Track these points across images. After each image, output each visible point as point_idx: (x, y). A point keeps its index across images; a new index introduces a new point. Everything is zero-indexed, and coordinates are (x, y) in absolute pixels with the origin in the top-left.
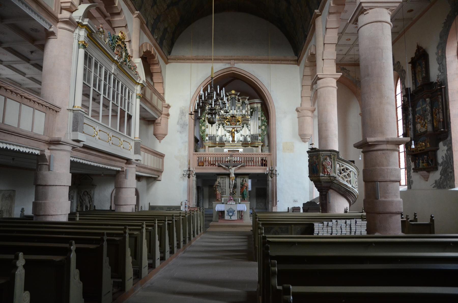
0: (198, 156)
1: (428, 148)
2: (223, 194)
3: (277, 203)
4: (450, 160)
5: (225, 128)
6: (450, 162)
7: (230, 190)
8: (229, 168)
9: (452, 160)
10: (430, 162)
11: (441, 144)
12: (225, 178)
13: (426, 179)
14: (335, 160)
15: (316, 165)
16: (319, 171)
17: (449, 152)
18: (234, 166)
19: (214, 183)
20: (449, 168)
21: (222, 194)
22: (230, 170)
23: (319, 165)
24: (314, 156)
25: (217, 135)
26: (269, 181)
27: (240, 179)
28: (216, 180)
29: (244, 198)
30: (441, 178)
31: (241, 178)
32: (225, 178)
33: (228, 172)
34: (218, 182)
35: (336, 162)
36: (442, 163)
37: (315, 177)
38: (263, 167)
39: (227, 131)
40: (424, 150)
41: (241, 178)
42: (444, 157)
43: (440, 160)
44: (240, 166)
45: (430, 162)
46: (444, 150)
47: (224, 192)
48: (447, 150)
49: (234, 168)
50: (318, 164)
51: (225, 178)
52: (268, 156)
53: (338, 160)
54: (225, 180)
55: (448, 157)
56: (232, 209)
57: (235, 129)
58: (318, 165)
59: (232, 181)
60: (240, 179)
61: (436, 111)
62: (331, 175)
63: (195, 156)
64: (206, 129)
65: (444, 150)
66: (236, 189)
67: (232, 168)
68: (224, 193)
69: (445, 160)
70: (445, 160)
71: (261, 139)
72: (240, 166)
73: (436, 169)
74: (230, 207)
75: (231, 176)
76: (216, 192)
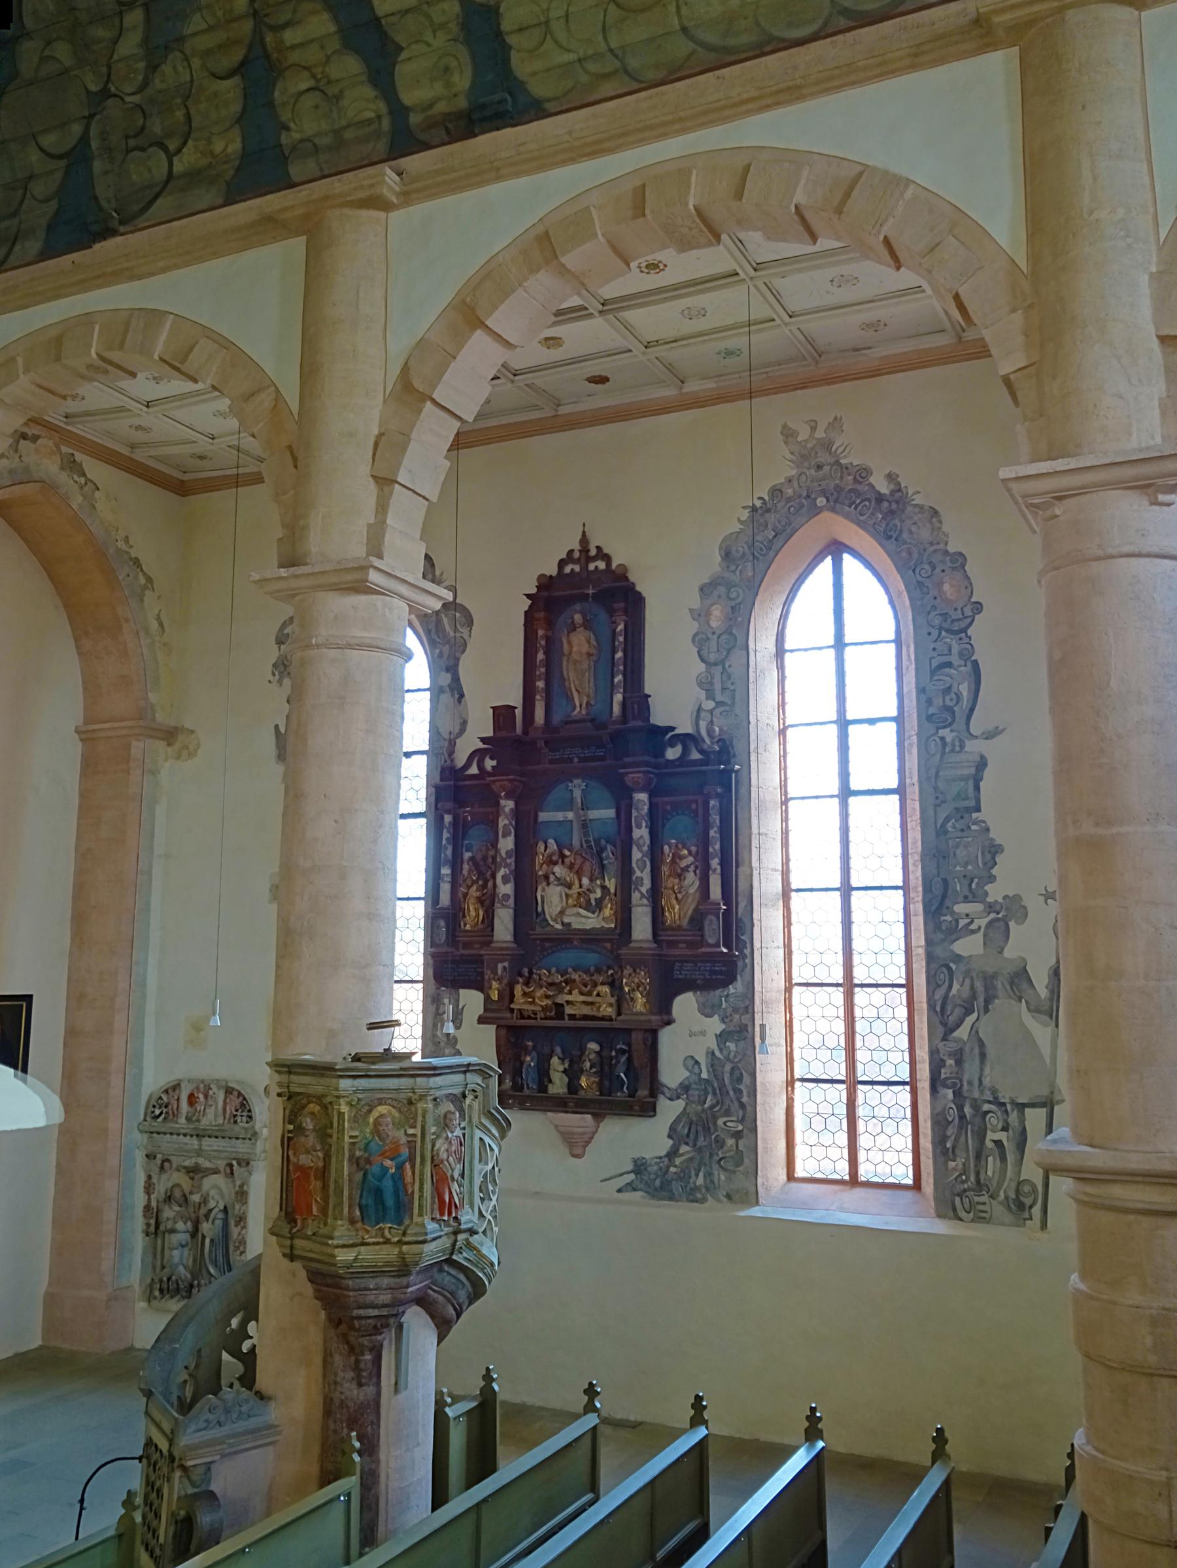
1: (637, 1014)
4: (740, 1080)
6: (739, 1092)
9: (747, 1079)
10: (622, 1075)
11: (685, 1004)
13: (576, 1145)
14: (475, 1120)
15: (400, 1167)
16: (416, 1211)
17: (731, 1046)
20: (727, 1113)
23: (418, 1160)
24: (381, 1102)
30: (672, 1154)
35: (478, 1134)
36: (685, 1088)
37: (387, 1242)
40: (610, 1019)
42: (697, 1062)
43: (671, 1073)
45: (622, 1075)
46: (703, 1033)
48: (722, 1037)
50: (412, 1159)
53: (485, 1121)
55: (728, 1067)
58: (408, 1165)
61: (677, 857)
62: (463, 1220)
65: (703, 1033)
69: (704, 1075)
70: (704, 1075)
73: (648, 1110)
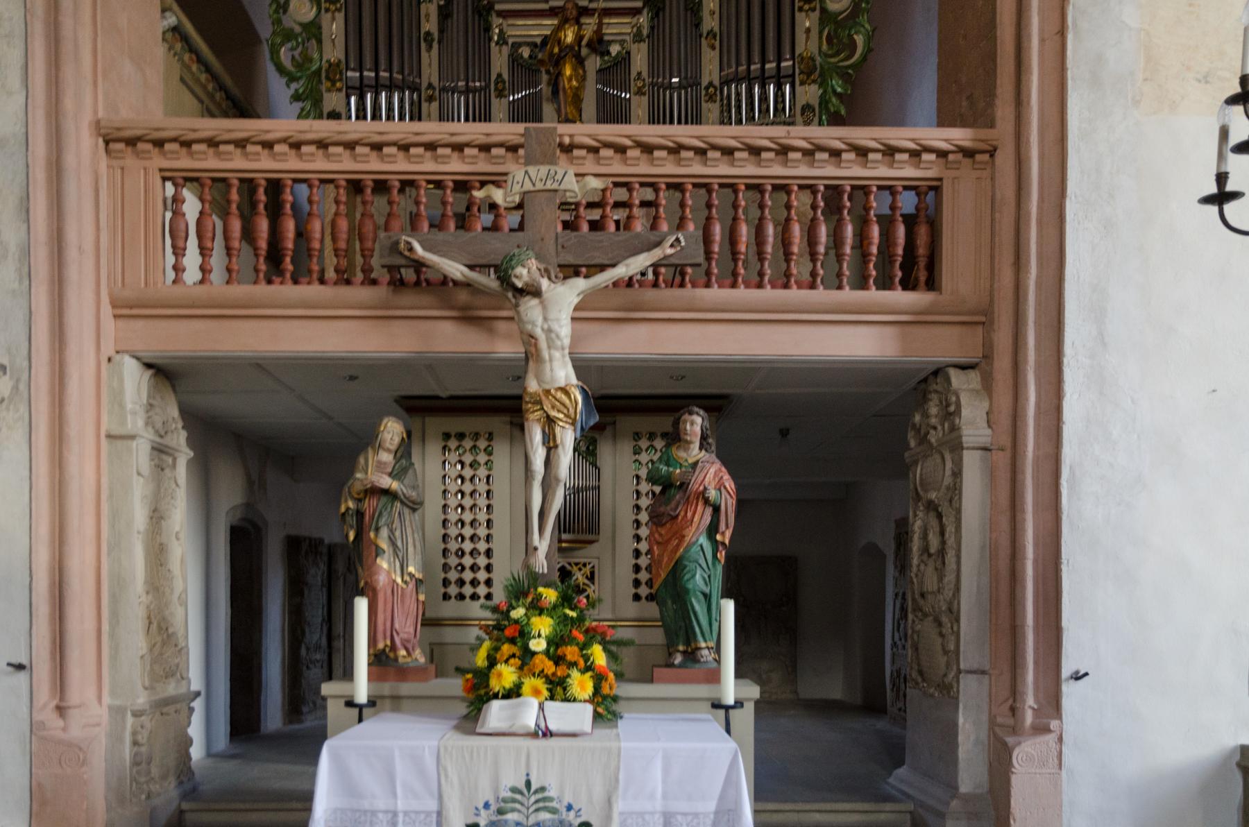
0: (158, 161)
2: (468, 590)
3: (1067, 703)
5: (496, 21)
7: (530, 550)
8: (505, 279)
12: (490, 437)
18: (571, 271)
19: (351, 469)
21: (446, 597)
22: (530, 307)
25: (430, 86)
26: (962, 448)
27: (637, 451)
28: (368, 439)
29: (690, 637)
31: (637, 436)
32: (482, 444)
33: (506, 348)
34: (387, 457)
38: (899, 297)
39: (516, 46)
41: (637, 436)
44: (641, 262)
47: (482, 576)
49: (580, 284)
51: (482, 444)
52: (948, 175)
54: (482, 458)
56: (544, 803)
57: (590, 23)
59: (551, 445)
60: (637, 451)
63: (130, 161)
64: (326, 18)
66: (593, 550)
67: (545, 283)
68: (474, 583)
71: (815, 102)
72: (641, 262)
74: (511, 778)
75: (533, 386)
76: (372, 569)
